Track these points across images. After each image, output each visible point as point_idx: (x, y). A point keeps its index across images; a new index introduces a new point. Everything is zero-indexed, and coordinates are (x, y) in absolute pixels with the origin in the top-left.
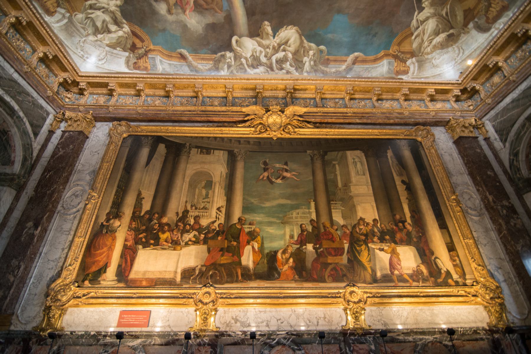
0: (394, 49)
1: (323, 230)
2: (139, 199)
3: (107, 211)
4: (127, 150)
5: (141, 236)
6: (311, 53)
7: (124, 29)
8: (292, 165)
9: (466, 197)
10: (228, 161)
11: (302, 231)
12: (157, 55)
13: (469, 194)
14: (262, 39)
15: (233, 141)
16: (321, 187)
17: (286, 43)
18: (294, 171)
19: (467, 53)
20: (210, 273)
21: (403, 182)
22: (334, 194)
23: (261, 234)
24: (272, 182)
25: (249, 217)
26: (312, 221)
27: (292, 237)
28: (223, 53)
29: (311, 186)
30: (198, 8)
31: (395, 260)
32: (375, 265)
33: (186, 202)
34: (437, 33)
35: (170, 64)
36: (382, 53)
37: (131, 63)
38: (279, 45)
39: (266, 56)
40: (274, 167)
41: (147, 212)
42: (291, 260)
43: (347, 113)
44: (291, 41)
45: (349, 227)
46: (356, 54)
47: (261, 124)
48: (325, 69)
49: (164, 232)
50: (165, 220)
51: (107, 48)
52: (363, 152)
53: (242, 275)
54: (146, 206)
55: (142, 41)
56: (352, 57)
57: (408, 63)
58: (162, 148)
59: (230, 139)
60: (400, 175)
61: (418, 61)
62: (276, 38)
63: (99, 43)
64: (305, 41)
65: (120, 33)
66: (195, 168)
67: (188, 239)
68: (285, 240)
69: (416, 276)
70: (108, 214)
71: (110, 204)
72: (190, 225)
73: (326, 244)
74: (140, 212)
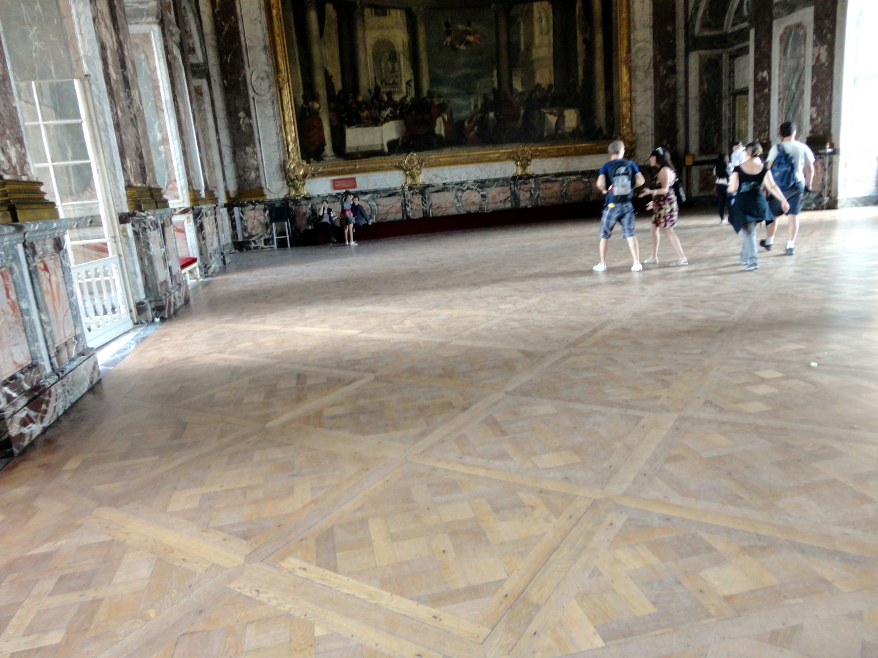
2: (328, 79)
3: (301, 93)
5: (343, 115)
8: (476, 26)
9: (640, 55)
10: (408, 25)
16: (504, 53)
21: (585, 41)
24: (455, 49)
26: (494, 90)
27: (476, 106)
33: (375, 78)
41: (340, 92)
42: (476, 128)
49: (363, 111)
50: (360, 99)
54: (338, 85)
60: (583, 32)
66: (374, 36)
69: (575, 135)
70: (304, 96)
71: (301, 87)
74: (334, 91)
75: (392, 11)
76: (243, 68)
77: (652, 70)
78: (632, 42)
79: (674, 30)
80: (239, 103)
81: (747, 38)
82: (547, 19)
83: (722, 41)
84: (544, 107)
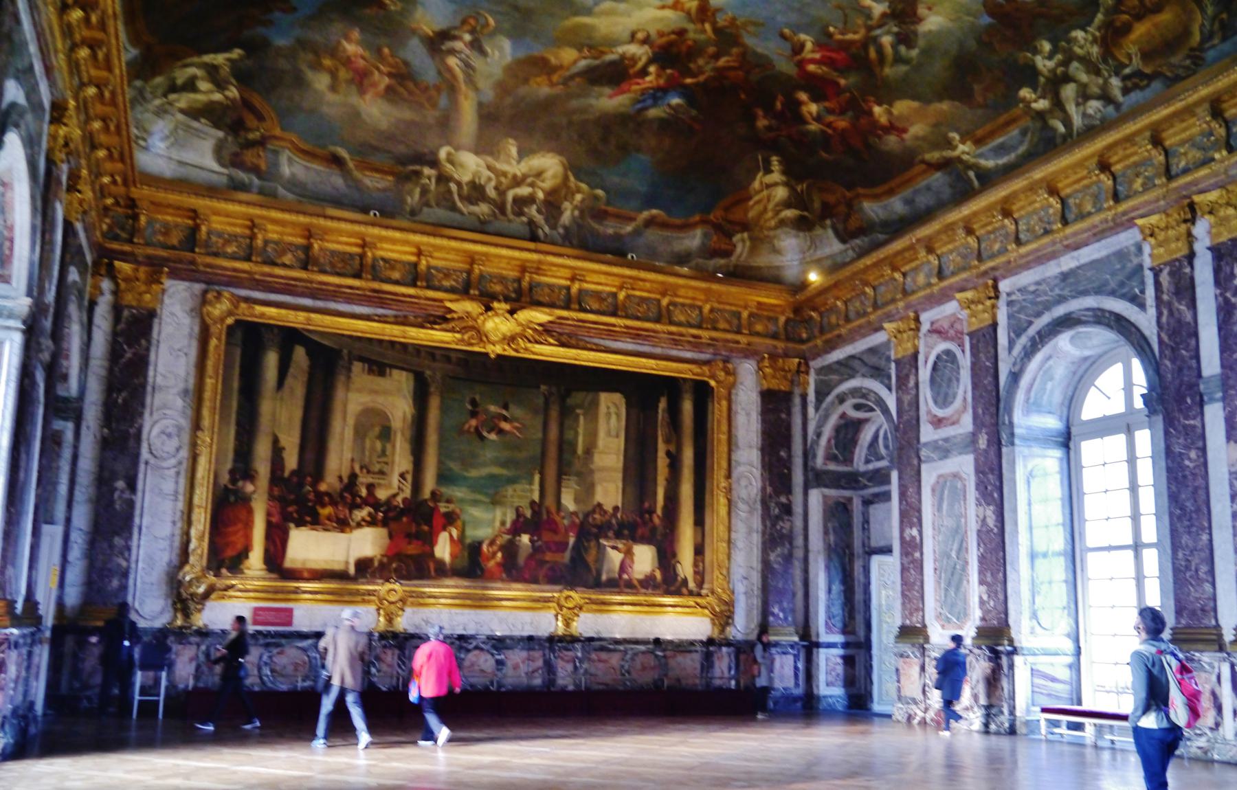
0: (716, 215)
1: (545, 517)
4: (238, 352)
6: (579, 197)
7: (227, 93)
8: (516, 411)
9: (743, 482)
11: (519, 514)
12: (283, 147)
13: (749, 479)
14: (497, 159)
15: (423, 354)
17: (539, 174)
18: (517, 420)
19: (820, 254)
20: (394, 565)
21: (668, 454)
22: (570, 464)
23: (464, 517)
24: (482, 438)
25: (446, 491)
26: (533, 503)
27: (503, 523)
28: (417, 168)
29: (538, 450)
30: (390, 94)
31: (628, 561)
32: (602, 565)
33: (353, 460)
34: (787, 204)
35: (307, 168)
36: (697, 218)
37: (226, 154)
38: (525, 177)
39: (496, 188)
40: (486, 411)
42: (499, 555)
43: (614, 325)
44: (549, 174)
45: (581, 516)
46: (654, 212)
47: (473, 328)
48: (596, 226)
51: (180, 117)
52: (626, 397)
53: (436, 571)
55: (261, 118)
56: (645, 214)
57: (737, 238)
58: (300, 353)
59: (418, 349)
61: (751, 238)
62: (523, 164)
63: (167, 107)
64: (572, 178)
65: (217, 97)
67: (359, 518)
68: (493, 527)
69: (648, 583)
72: (361, 497)
73: (547, 536)
75: (396, 372)
76: (141, 415)
77: (759, 506)
78: (733, 463)
79: (790, 456)
80: (119, 467)
81: (887, 480)
82: (618, 415)
83: (851, 480)
84: (606, 537)
